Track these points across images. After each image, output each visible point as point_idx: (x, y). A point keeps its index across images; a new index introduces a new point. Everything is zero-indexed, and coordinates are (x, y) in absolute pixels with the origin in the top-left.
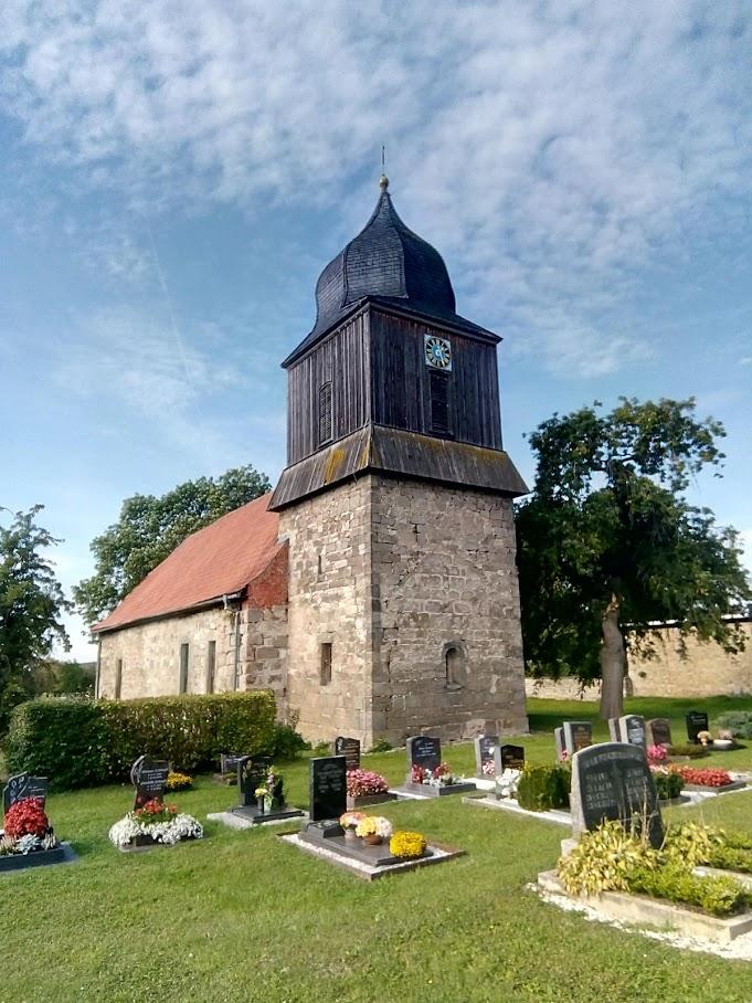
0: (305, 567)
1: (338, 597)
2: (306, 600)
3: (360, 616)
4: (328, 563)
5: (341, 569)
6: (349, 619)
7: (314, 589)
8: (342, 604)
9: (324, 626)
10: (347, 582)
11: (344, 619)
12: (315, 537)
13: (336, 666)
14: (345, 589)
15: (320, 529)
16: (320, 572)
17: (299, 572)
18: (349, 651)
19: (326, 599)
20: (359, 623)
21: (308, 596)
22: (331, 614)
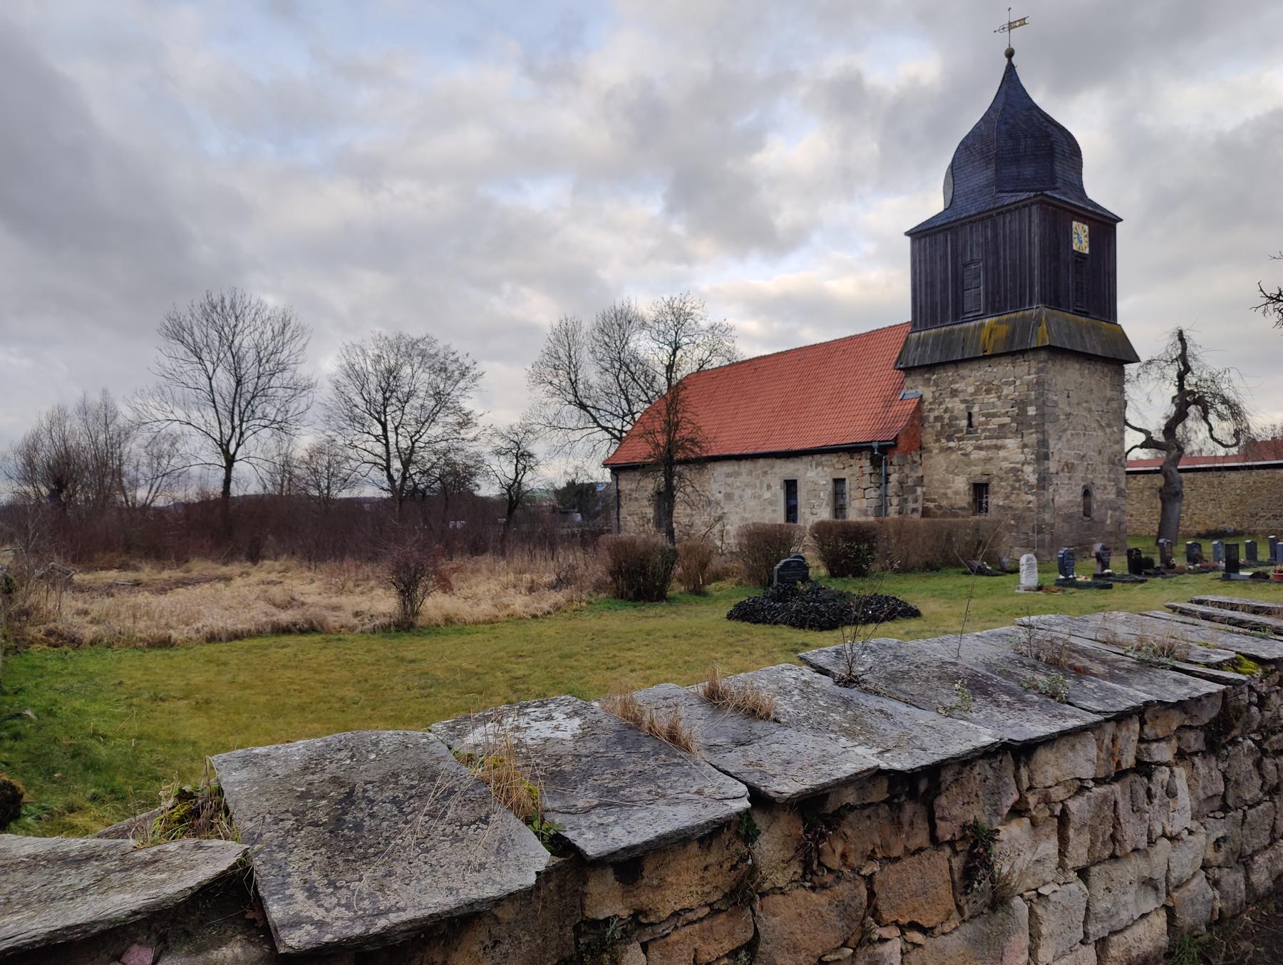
0: (946, 421)
1: (998, 448)
2: (950, 448)
3: (1029, 464)
4: (983, 419)
5: (1002, 426)
6: (1013, 465)
7: (960, 439)
8: (1002, 453)
9: (977, 470)
10: (1010, 435)
11: (1006, 465)
12: (961, 396)
13: (995, 500)
14: (1007, 441)
15: (971, 389)
16: (970, 425)
17: (938, 425)
18: (1013, 488)
19: (979, 448)
20: (1028, 469)
21: (952, 444)
22: (988, 460)
